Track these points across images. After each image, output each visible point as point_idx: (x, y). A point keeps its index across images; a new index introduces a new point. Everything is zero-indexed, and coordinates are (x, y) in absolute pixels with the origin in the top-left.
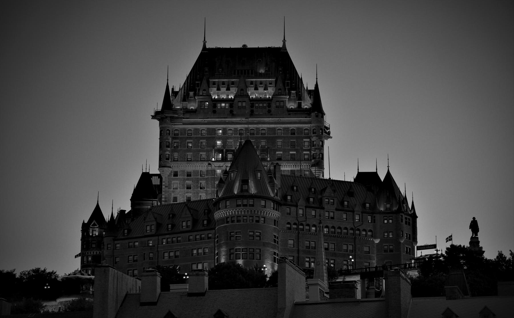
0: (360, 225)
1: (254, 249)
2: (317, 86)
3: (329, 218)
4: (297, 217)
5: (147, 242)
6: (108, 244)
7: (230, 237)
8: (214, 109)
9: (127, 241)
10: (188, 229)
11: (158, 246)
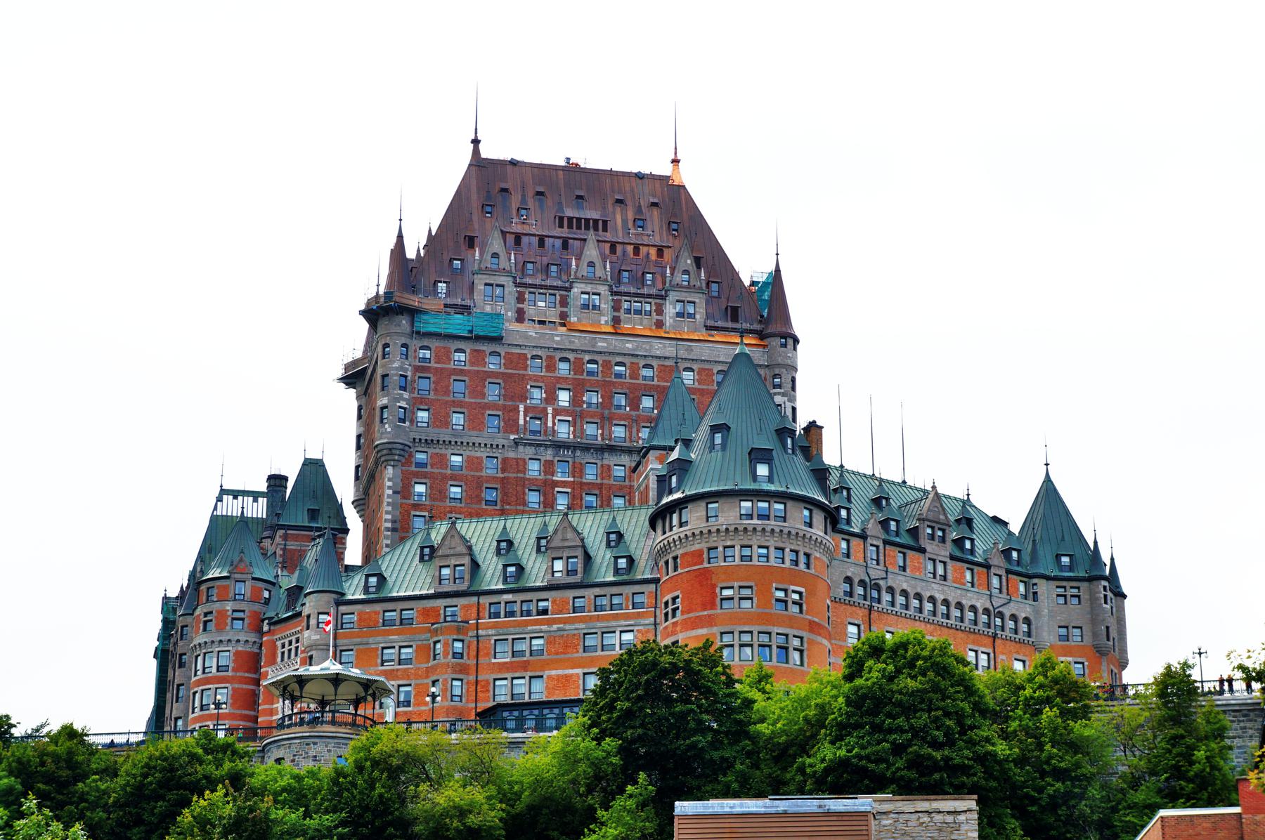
0: (1004, 604)
1: (787, 635)
2: (778, 271)
3: (935, 577)
4: (866, 567)
5: (442, 612)
6: (319, 613)
7: (722, 599)
8: (521, 306)
9: (378, 607)
10: (571, 580)
11: (477, 623)
